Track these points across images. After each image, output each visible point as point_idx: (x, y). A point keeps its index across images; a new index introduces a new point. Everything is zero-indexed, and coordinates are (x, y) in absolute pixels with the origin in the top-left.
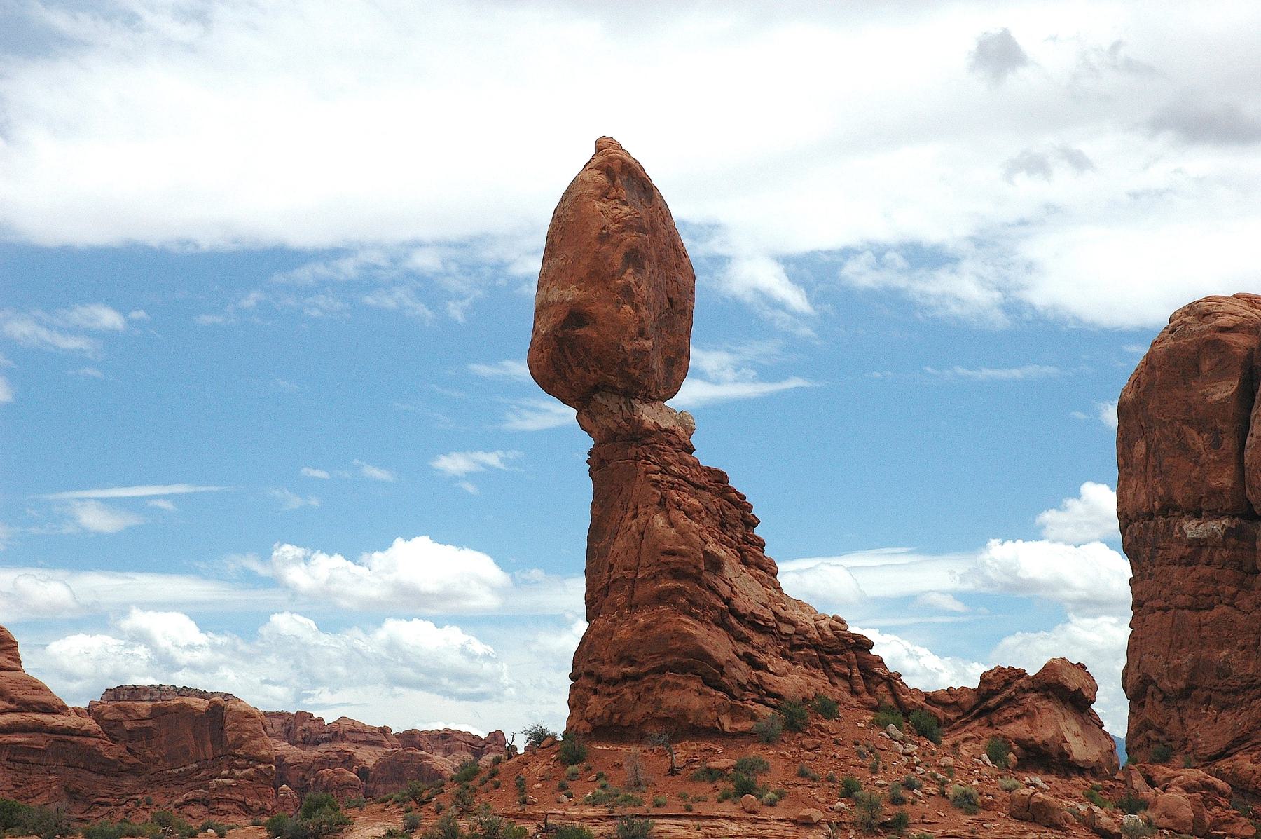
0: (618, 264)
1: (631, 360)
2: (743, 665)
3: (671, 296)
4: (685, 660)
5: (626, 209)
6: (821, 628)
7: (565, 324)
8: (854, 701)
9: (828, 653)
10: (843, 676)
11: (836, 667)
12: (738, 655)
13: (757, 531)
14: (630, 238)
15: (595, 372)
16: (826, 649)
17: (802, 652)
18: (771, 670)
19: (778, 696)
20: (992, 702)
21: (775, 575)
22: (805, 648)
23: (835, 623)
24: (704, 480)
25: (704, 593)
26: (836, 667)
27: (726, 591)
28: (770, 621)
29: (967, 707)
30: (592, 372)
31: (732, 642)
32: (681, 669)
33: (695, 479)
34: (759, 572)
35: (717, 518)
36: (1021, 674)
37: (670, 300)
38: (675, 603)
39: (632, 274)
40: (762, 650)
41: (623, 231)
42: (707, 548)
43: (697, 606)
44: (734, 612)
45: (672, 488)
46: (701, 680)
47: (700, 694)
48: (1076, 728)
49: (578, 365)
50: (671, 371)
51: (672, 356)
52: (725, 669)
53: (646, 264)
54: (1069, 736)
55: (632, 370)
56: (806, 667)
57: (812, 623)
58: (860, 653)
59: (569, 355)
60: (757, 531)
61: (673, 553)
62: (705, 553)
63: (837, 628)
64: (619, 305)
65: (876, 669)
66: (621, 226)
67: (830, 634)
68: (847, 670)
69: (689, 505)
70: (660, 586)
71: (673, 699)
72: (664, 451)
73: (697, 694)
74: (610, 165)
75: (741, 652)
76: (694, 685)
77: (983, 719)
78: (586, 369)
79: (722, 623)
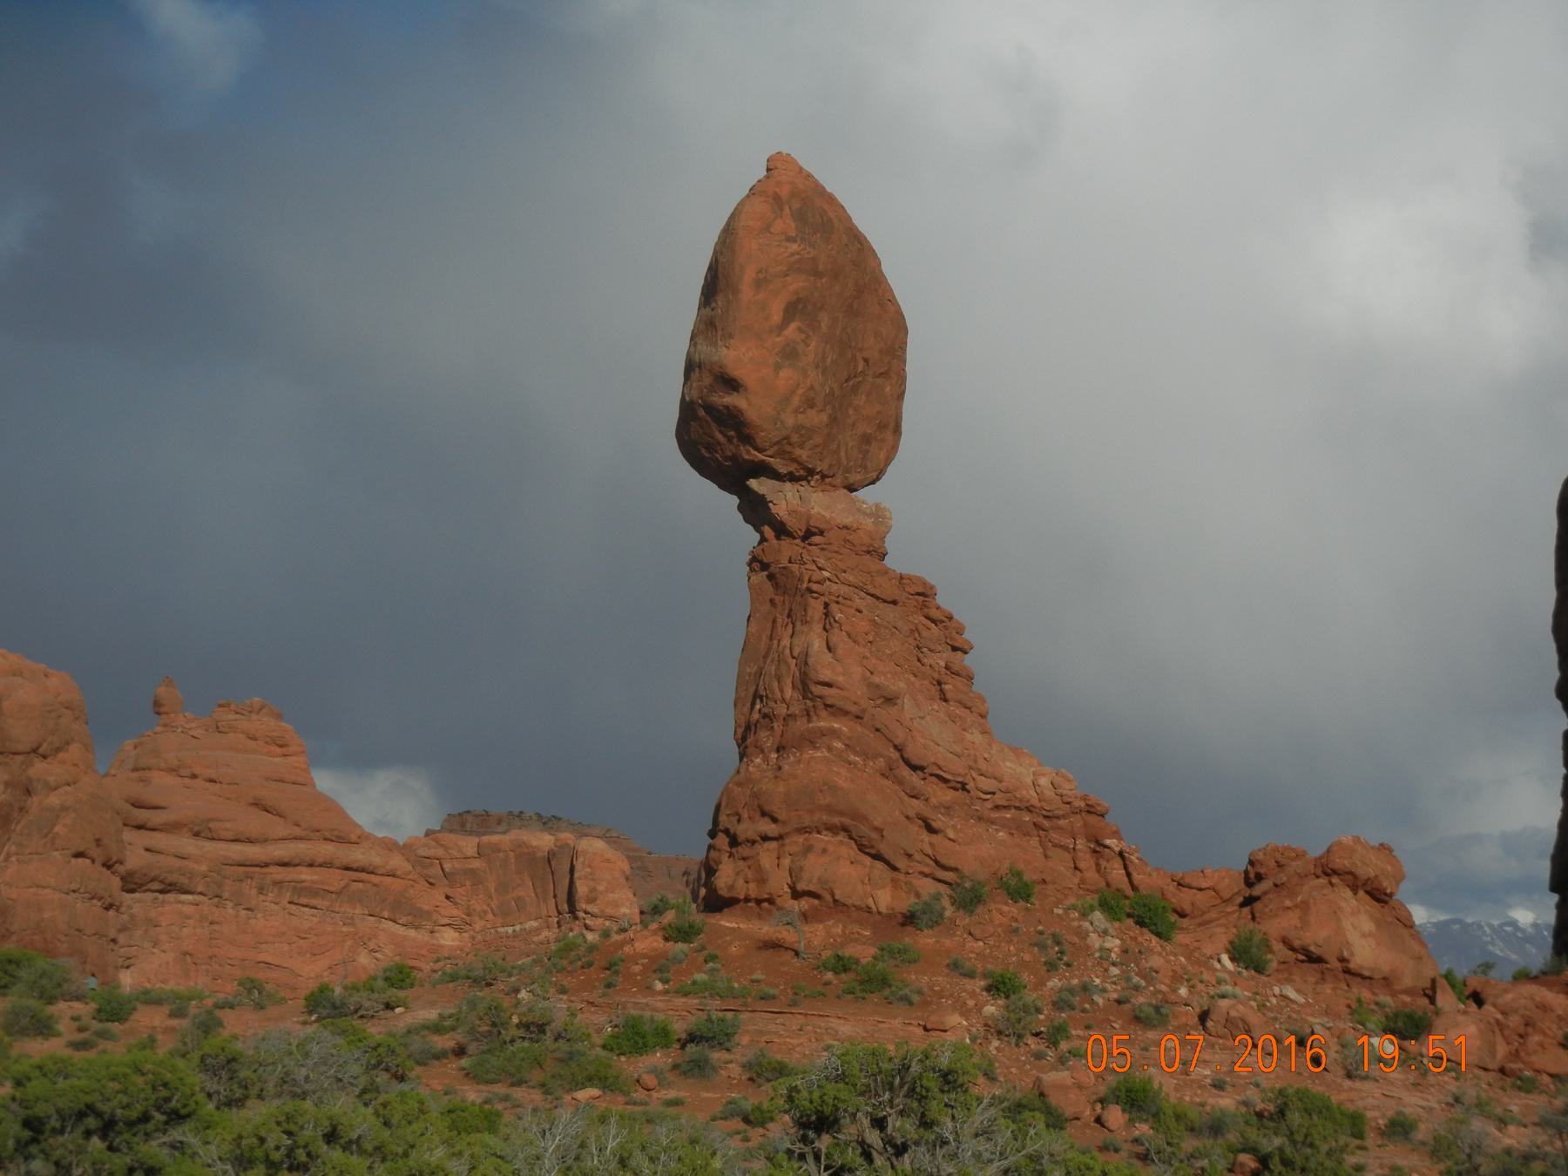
0: (777, 318)
1: (795, 438)
2: (916, 829)
3: (866, 354)
4: (836, 820)
5: (794, 247)
6: (1039, 786)
7: (711, 389)
8: (1073, 881)
9: (1046, 817)
10: (1066, 849)
11: (1054, 835)
12: (907, 817)
13: (969, 660)
14: (798, 283)
16: (1044, 813)
17: (1008, 816)
18: (951, 835)
19: (955, 870)
20: (1257, 891)
21: (983, 716)
22: (1013, 811)
23: (1058, 780)
24: (890, 590)
26: (1054, 835)
27: (900, 736)
29: (1226, 895)
31: (902, 801)
32: (833, 829)
34: (960, 711)
35: (911, 640)
36: (1300, 855)
37: (866, 360)
38: (830, 749)
39: (799, 329)
40: (948, 809)
41: (787, 275)
42: (876, 679)
43: (856, 753)
44: (907, 763)
45: (838, 603)
46: (855, 847)
47: (852, 863)
48: (1367, 925)
50: (868, 451)
51: (869, 431)
52: (885, 833)
53: (824, 319)
54: (1353, 936)
55: (798, 452)
57: (1029, 780)
58: (1092, 819)
60: (969, 660)
61: (829, 685)
62: (870, 685)
64: (778, 367)
65: (1108, 842)
66: (785, 269)
67: (1049, 793)
68: (1069, 842)
70: (811, 725)
71: (814, 871)
72: (836, 552)
73: (848, 862)
74: (777, 190)
75: (912, 814)
76: (849, 850)
77: (1246, 910)
79: (888, 773)
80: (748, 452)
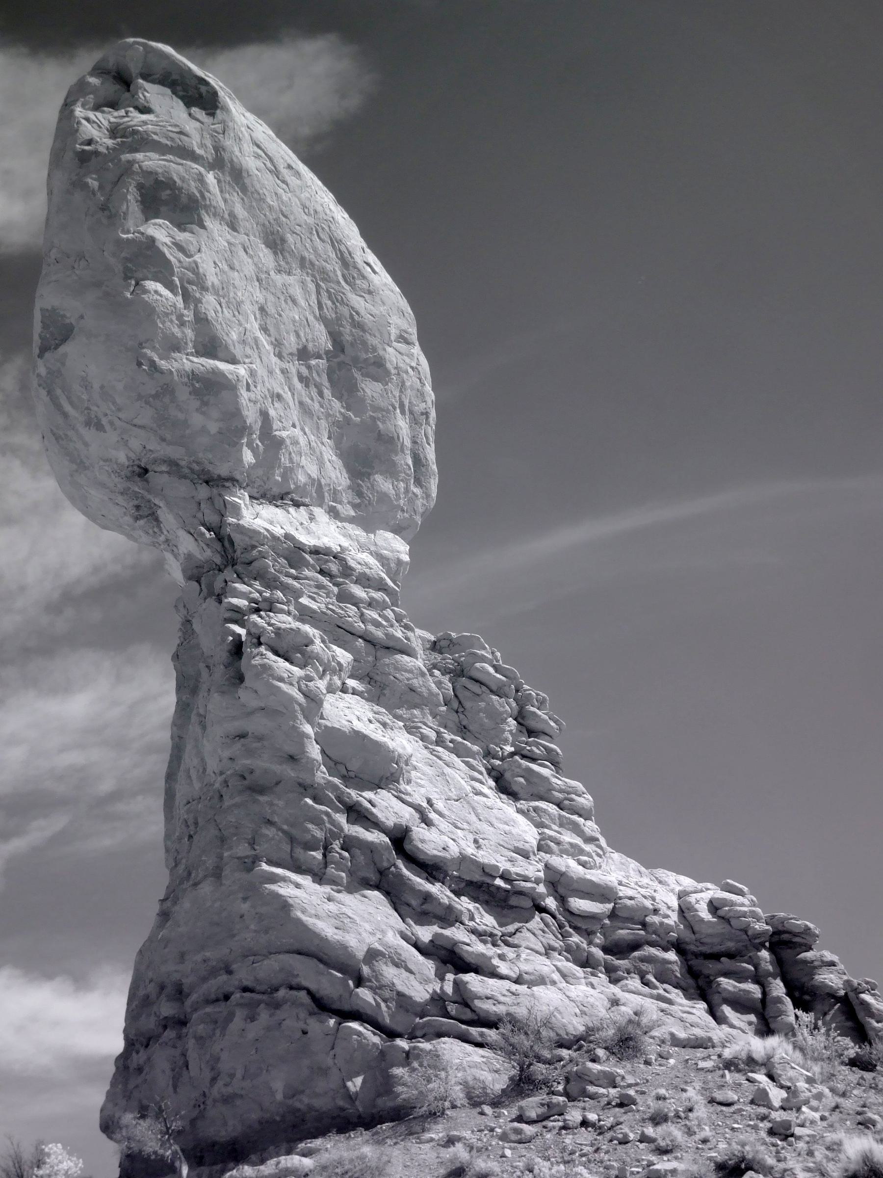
11: (727, 984)
12: (416, 946)
15: (111, 423)
18: (503, 968)
25: (327, 814)
28: (526, 879)
30: (108, 427)
33: (371, 628)
49: (88, 424)
52: (366, 970)
56: (646, 983)
57: (674, 903)
59: (68, 408)
63: (725, 902)
69: (278, 632)
78: (99, 427)
80: (111, 423)
